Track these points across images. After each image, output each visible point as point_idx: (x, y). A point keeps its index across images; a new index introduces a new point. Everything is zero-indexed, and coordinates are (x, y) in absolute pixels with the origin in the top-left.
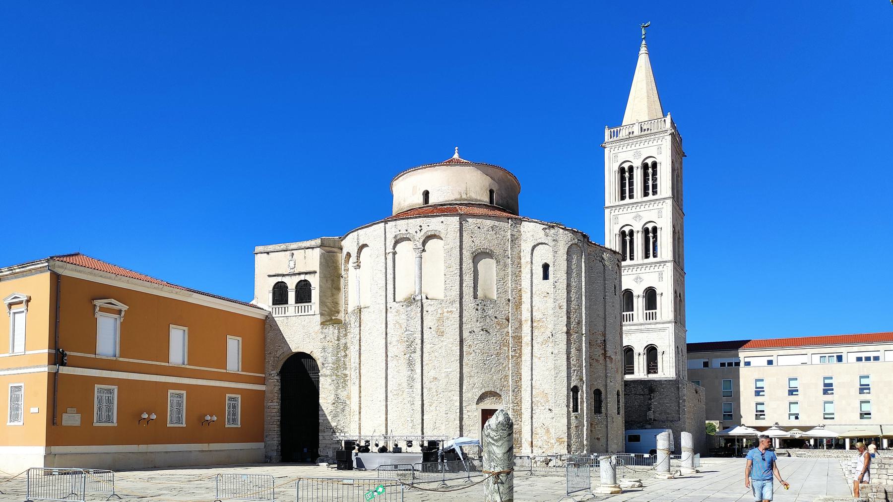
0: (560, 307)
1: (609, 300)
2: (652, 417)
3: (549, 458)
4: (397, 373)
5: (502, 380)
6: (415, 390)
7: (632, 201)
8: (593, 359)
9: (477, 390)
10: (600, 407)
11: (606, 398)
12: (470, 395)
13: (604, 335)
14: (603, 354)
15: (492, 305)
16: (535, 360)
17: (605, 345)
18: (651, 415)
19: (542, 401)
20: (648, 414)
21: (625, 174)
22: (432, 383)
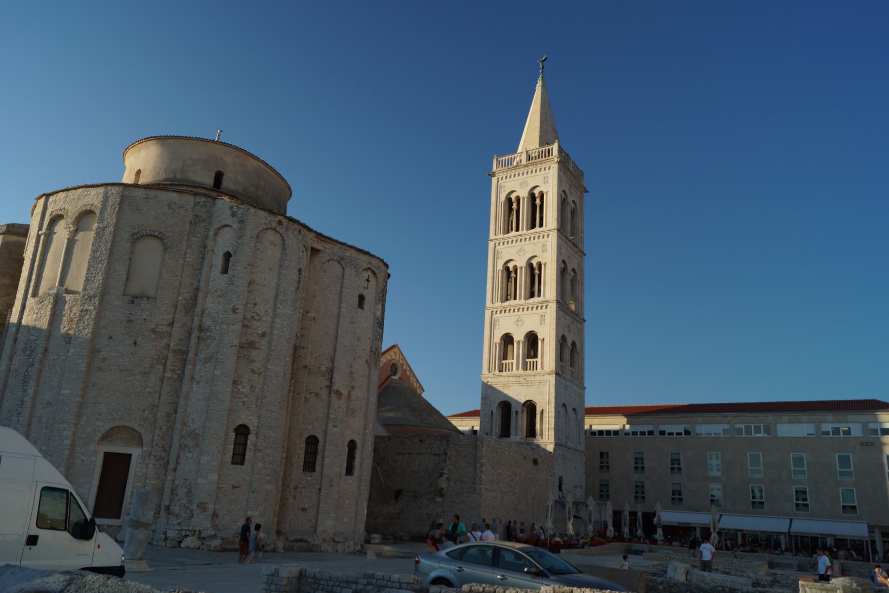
0: (234, 311)
1: (346, 314)
2: (444, 485)
3: (184, 533)
4: (11, 395)
5: (147, 412)
6: (21, 419)
7: (518, 233)
8: (311, 393)
9: (102, 424)
10: (314, 463)
11: (324, 450)
12: (90, 430)
13: (333, 360)
14: (327, 386)
15: (148, 306)
16: (194, 385)
17: (332, 375)
18: (443, 483)
19: (190, 445)
20: (439, 482)
21: (510, 204)
22: (45, 409)
